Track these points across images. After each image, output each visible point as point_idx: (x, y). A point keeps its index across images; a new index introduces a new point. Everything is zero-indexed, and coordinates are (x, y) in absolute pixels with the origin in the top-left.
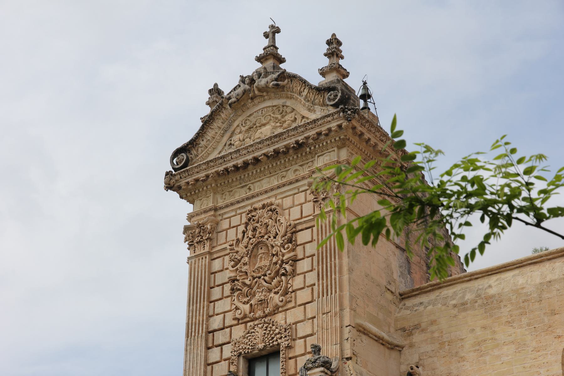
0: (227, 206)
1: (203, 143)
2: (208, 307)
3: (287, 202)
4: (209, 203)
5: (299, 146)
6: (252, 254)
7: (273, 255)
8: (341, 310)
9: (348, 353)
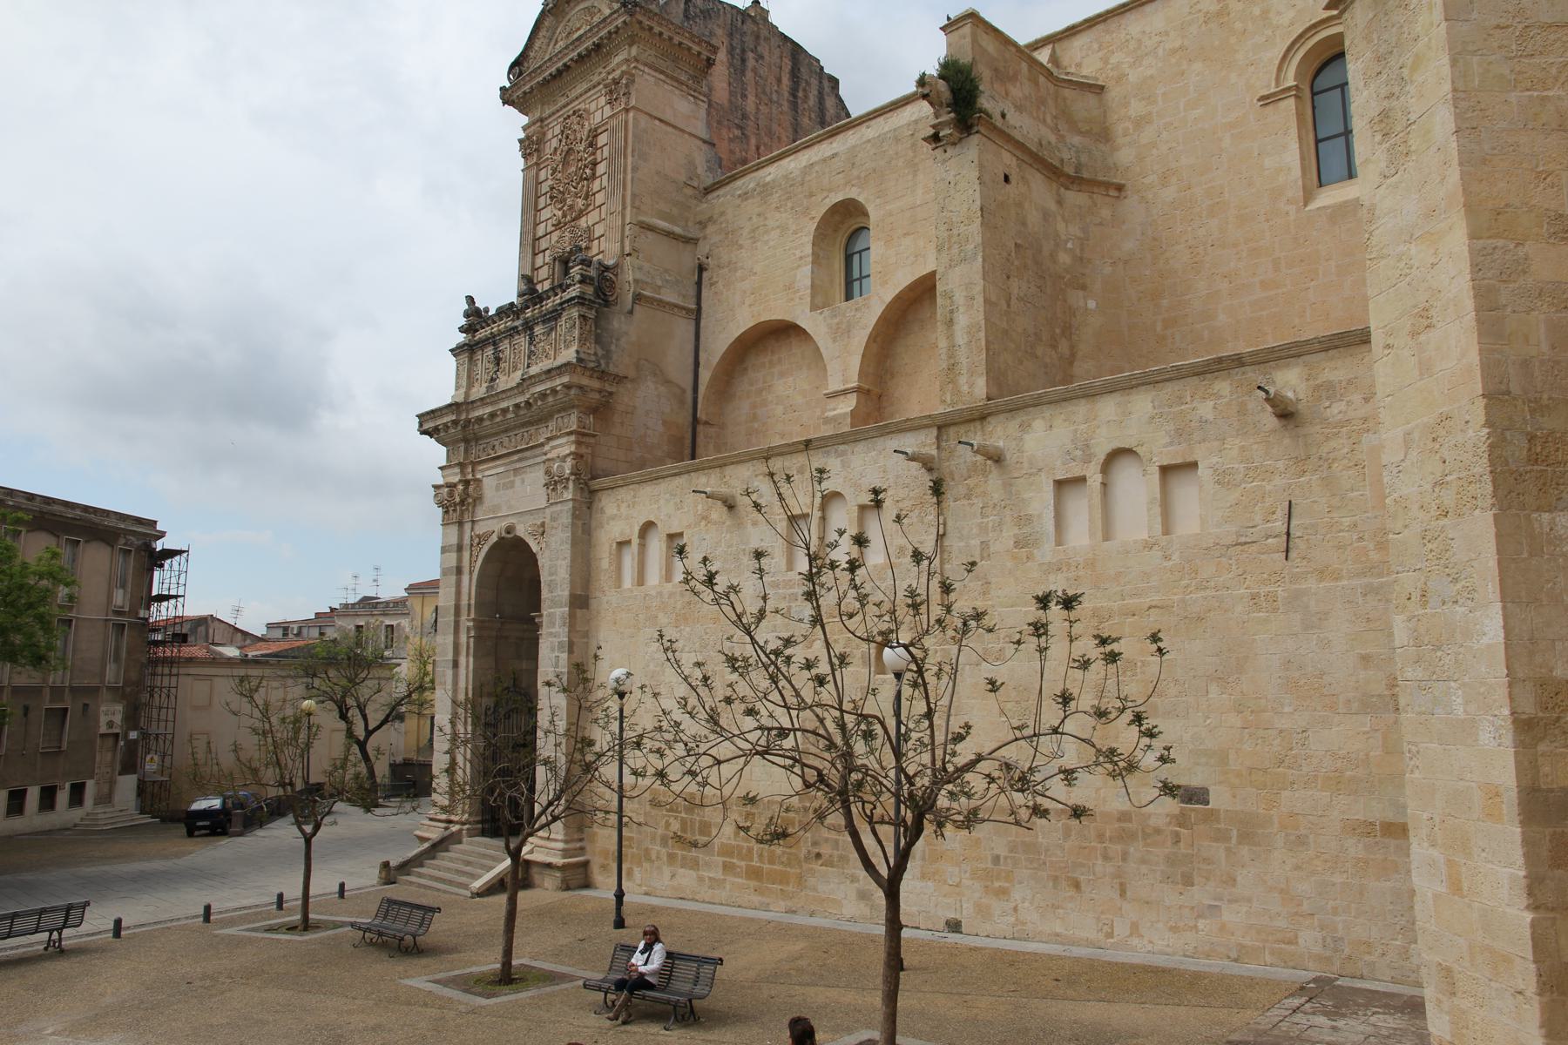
0: (550, 116)
1: (532, 54)
2: (535, 215)
3: (593, 107)
4: (537, 115)
5: (598, 47)
6: (565, 162)
7: (579, 160)
8: (624, 208)
9: (627, 250)
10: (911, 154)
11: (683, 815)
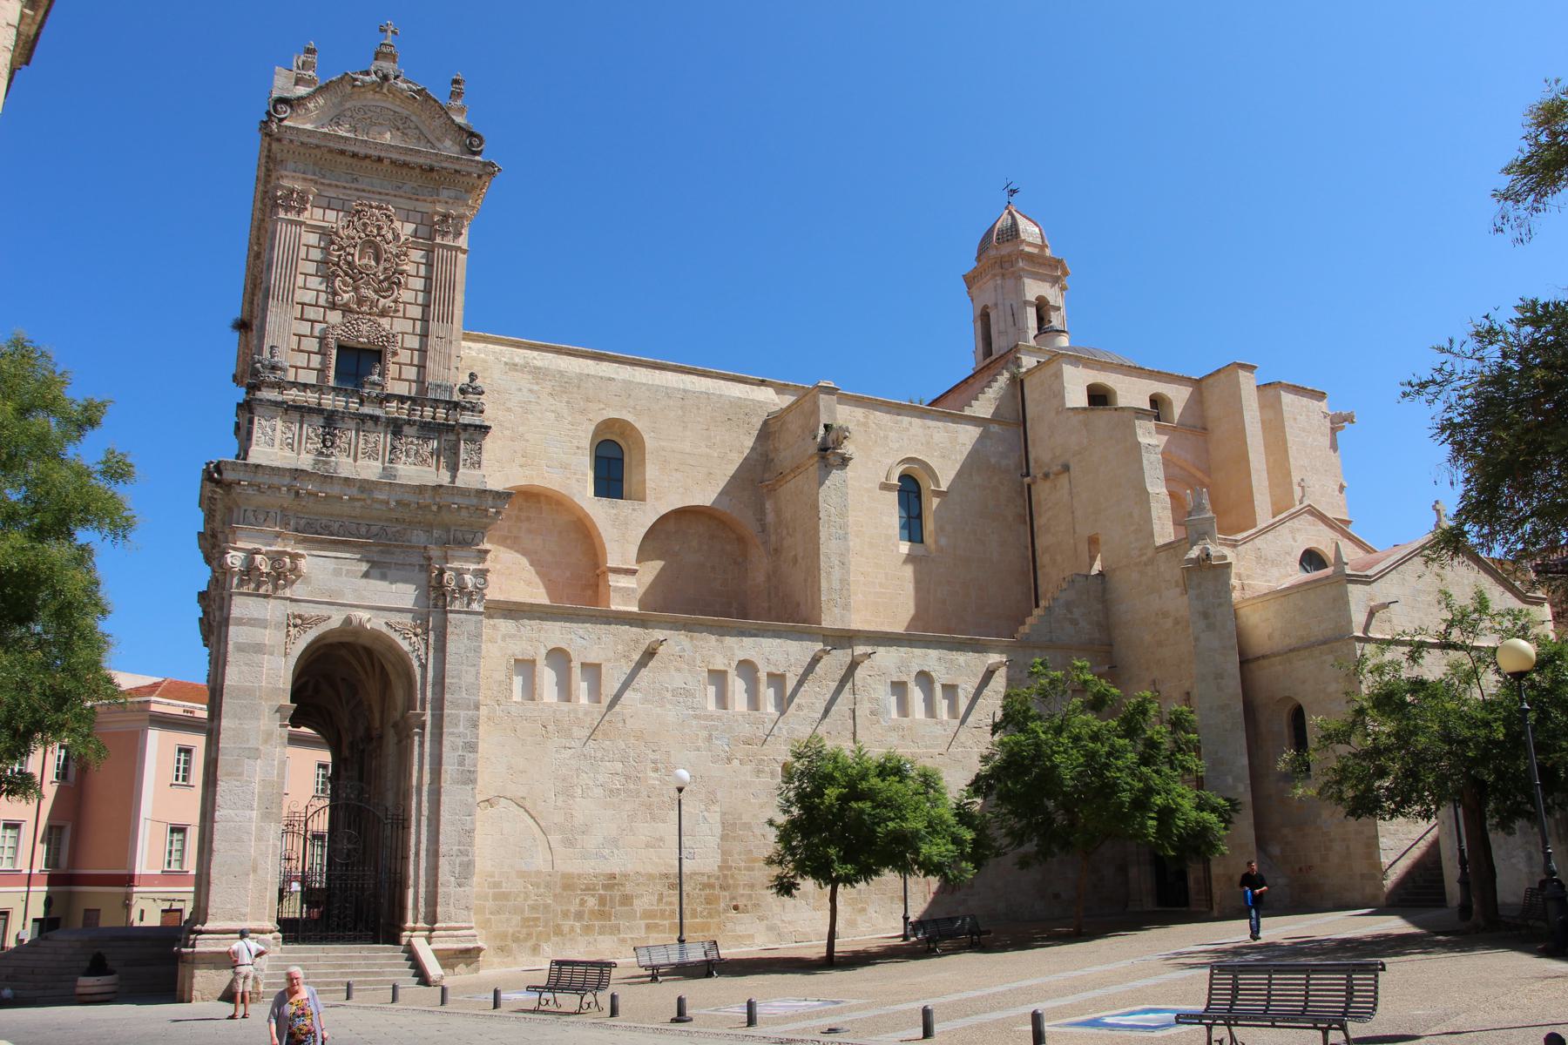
10: (680, 412)
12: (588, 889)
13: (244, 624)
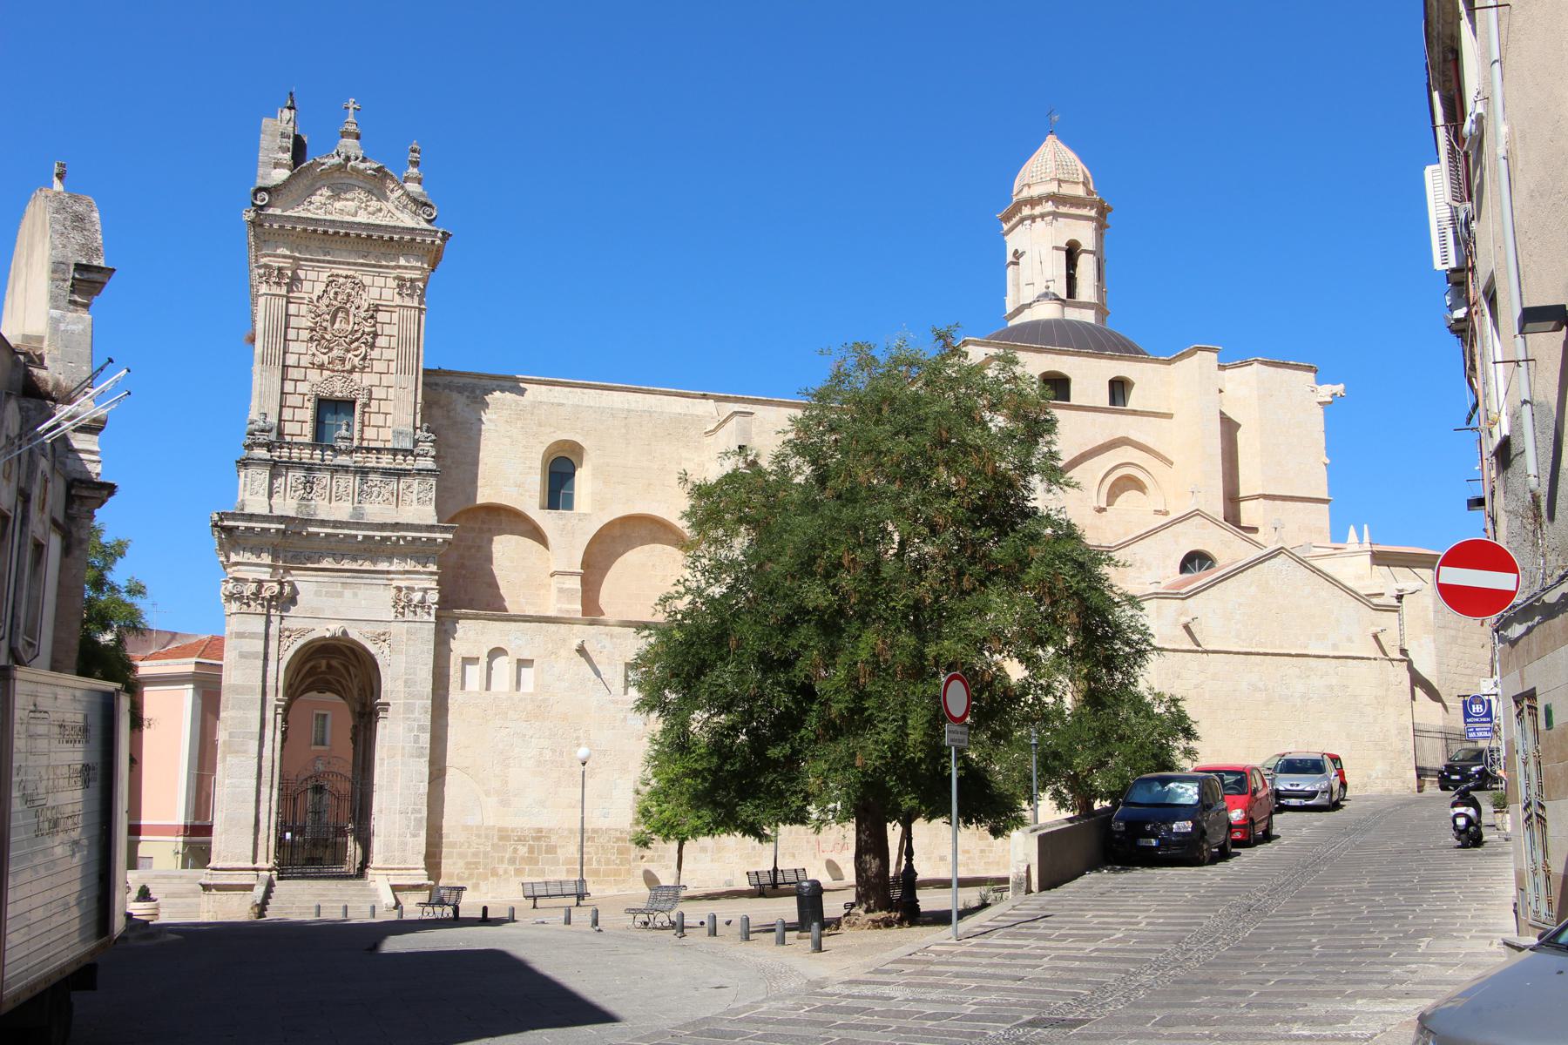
10: (623, 431)
11: (531, 842)
12: (520, 840)
13: (246, 637)
